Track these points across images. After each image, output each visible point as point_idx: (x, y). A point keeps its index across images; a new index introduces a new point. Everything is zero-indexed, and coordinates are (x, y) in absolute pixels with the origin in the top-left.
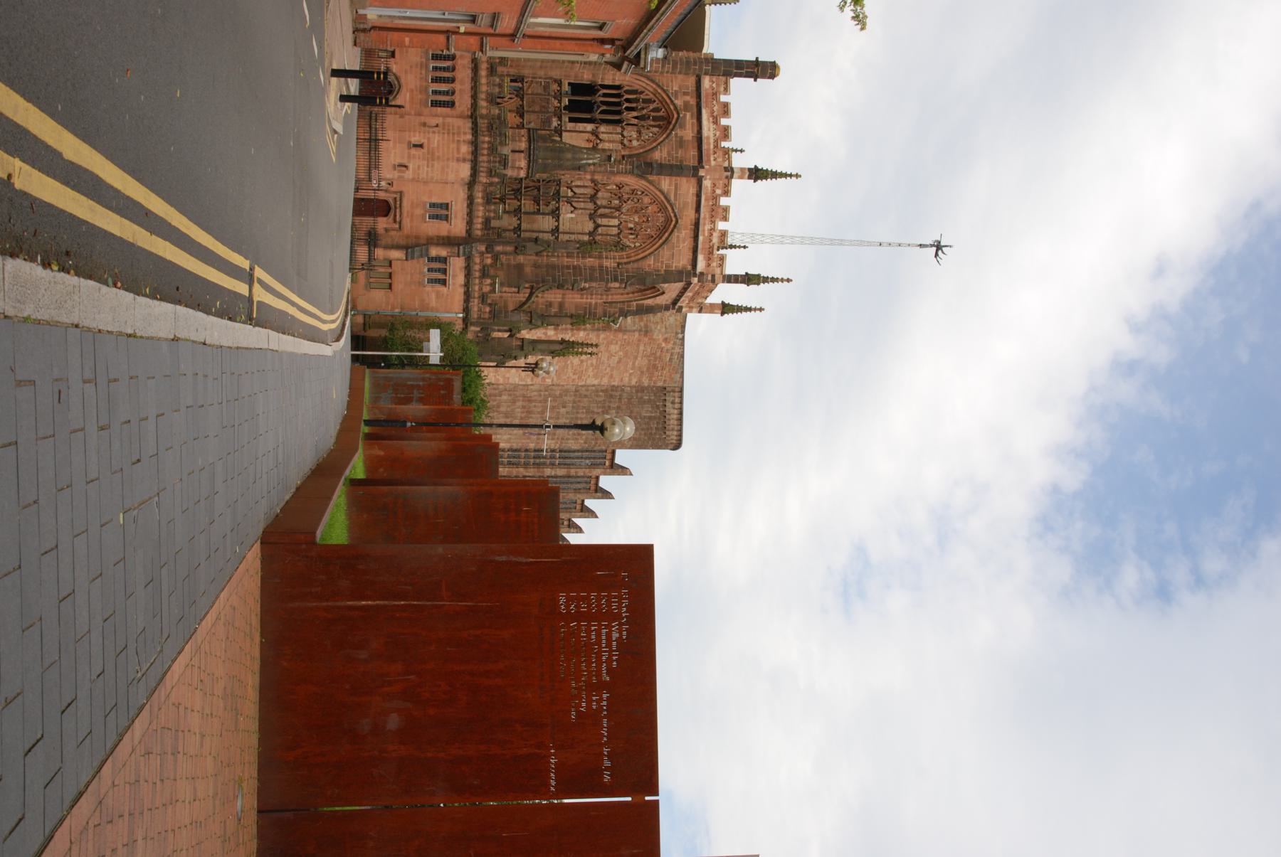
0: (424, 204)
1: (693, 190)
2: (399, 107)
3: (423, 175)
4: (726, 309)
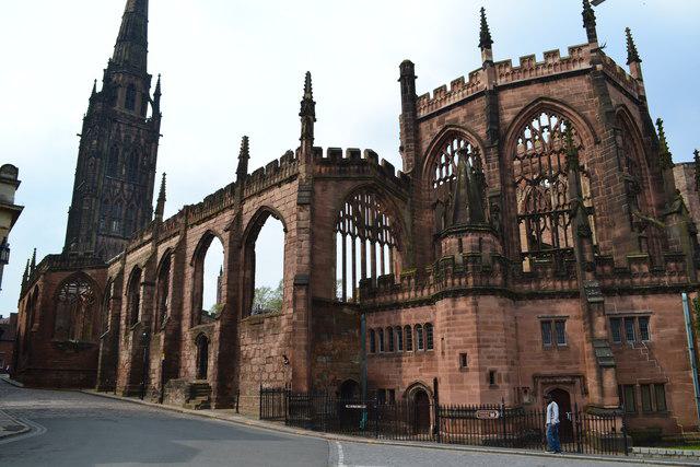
0: (545, 349)
1: (509, 93)
2: (436, 382)
3: (501, 352)
4: (633, 57)
